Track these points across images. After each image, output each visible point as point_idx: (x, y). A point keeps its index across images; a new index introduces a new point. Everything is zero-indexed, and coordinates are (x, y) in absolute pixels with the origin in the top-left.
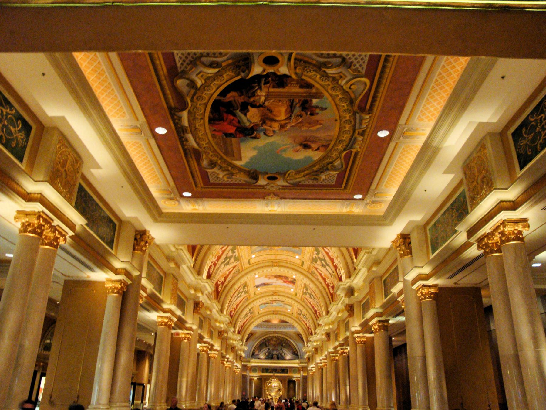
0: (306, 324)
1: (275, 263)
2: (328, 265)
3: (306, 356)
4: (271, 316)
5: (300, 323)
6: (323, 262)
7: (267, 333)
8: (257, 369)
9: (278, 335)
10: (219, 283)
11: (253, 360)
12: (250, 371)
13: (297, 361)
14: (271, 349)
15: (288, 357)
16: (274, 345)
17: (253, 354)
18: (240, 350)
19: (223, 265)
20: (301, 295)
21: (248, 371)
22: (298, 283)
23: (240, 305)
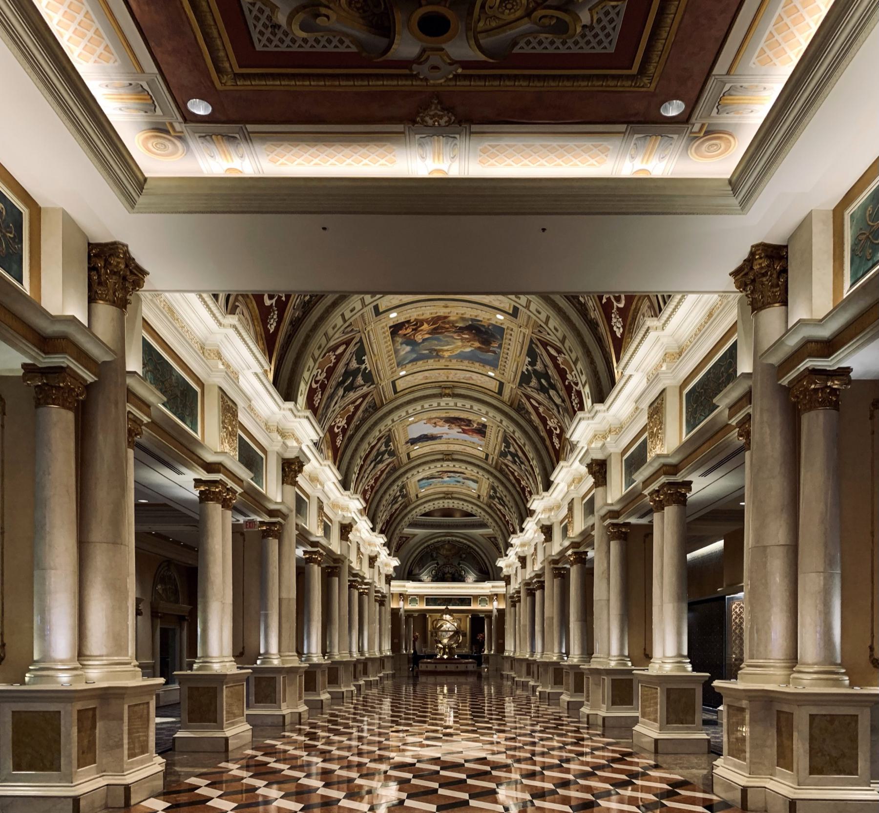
0: (504, 516)
1: (448, 390)
2: (553, 387)
5: (493, 514)
6: (543, 381)
10: (336, 430)
14: (441, 563)
16: (446, 557)
19: (341, 392)
20: (496, 457)
22: (491, 433)
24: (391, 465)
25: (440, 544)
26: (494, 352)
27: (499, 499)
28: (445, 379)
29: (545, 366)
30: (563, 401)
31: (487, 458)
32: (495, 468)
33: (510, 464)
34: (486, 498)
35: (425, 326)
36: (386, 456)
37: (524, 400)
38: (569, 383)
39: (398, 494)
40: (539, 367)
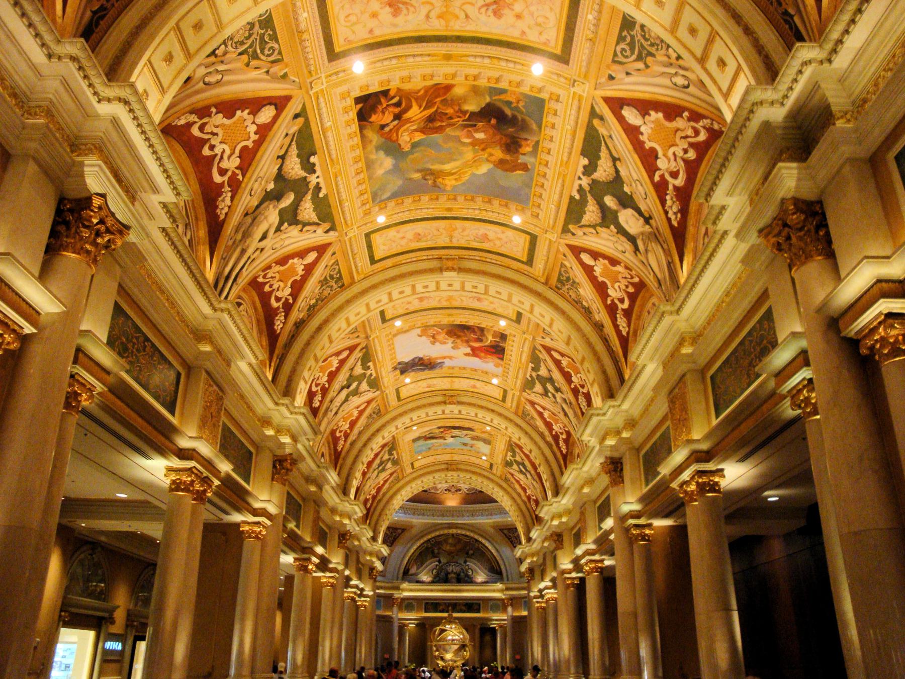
1: (448, 259)
3: (524, 568)
4: (443, 474)
5: (509, 489)
7: (436, 527)
8: (415, 603)
9: (459, 531)
11: (405, 585)
12: (400, 609)
13: (499, 586)
14: (443, 560)
15: (480, 578)
16: (450, 553)
17: (406, 572)
18: (371, 554)
20: (517, 393)
21: (395, 608)
23: (384, 490)
24: (373, 405)
25: (442, 538)
26: (525, 167)
27: (518, 463)
29: (615, 160)
30: (647, 220)
31: (504, 397)
32: (516, 413)
33: (538, 399)
34: (500, 467)
35: (415, 112)
36: (364, 386)
37: (571, 262)
38: (662, 176)
39: (386, 457)
40: (604, 171)
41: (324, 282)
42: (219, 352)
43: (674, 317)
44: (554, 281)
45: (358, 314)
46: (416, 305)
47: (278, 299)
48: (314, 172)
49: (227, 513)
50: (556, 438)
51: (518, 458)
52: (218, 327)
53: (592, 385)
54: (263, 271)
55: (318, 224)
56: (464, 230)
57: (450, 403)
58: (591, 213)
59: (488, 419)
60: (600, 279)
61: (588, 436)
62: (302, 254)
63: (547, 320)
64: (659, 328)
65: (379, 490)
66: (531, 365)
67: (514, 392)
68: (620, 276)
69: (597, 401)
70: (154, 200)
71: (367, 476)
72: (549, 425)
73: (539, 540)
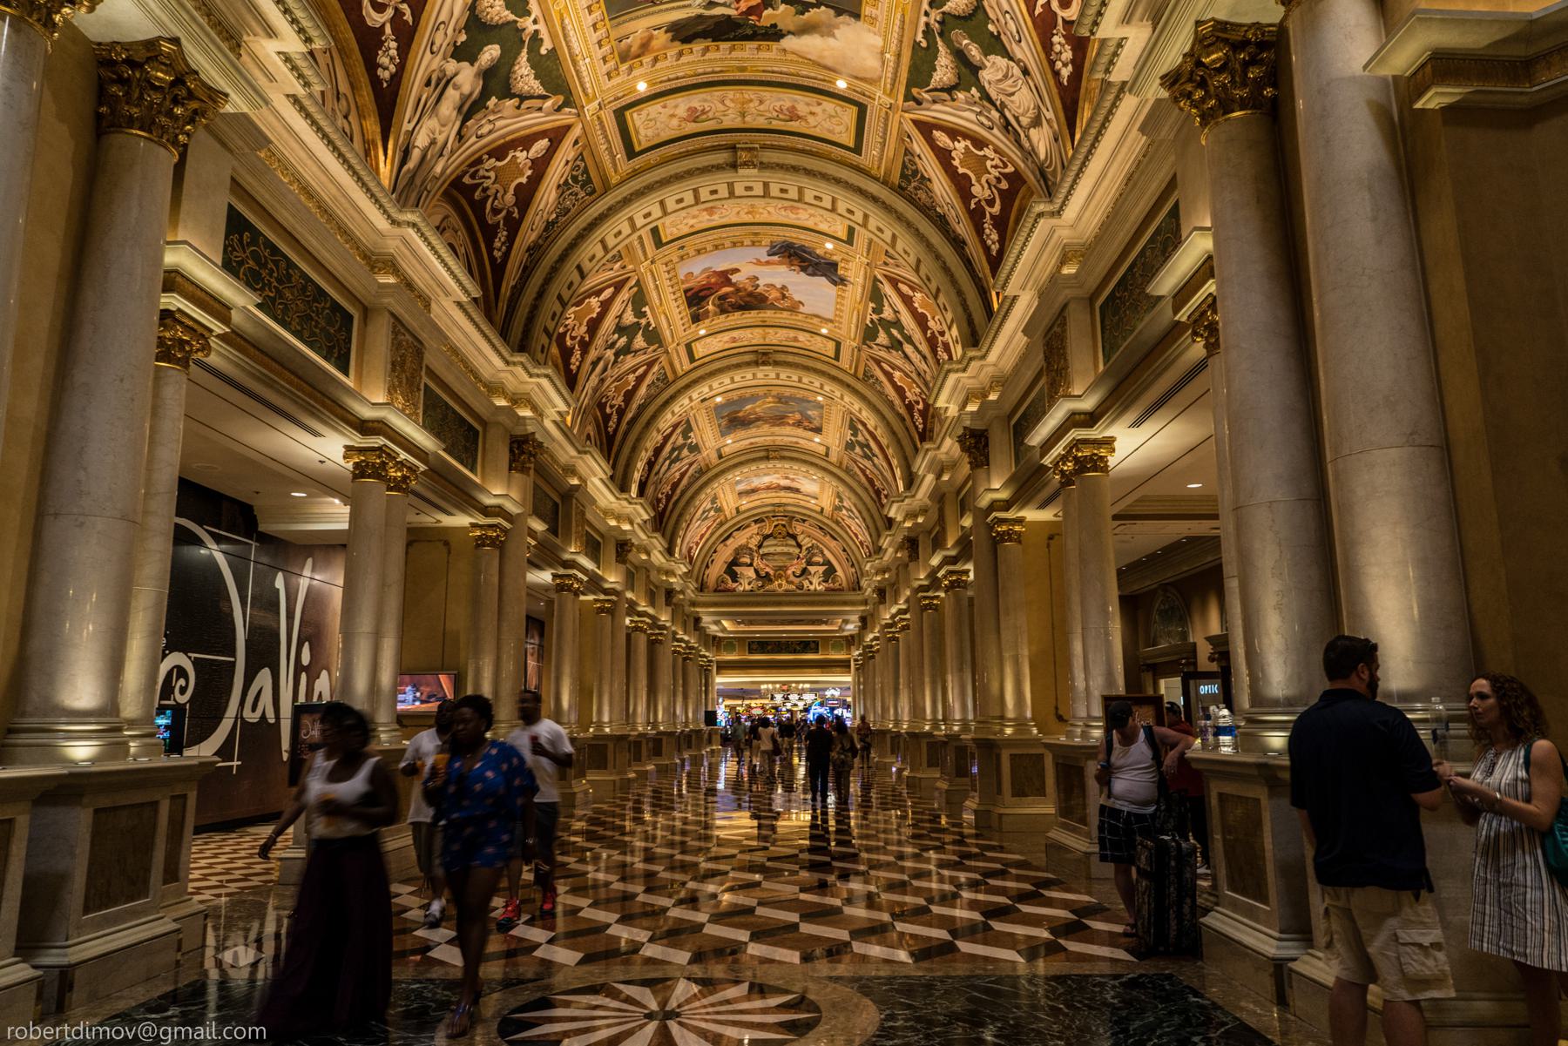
0: (871, 482)
27: (862, 446)
28: (738, 123)
32: (855, 376)
33: (883, 354)
36: (639, 341)
37: (919, 146)
39: (681, 441)
41: (563, 187)
42: (409, 285)
43: (1054, 221)
44: (895, 178)
45: (620, 233)
46: (704, 220)
47: (496, 211)
48: (529, 14)
49: (449, 514)
50: (910, 407)
51: (860, 438)
52: (403, 248)
53: (950, 328)
54: (470, 166)
55: (544, 98)
56: (761, 102)
57: (764, 363)
58: (944, 70)
59: (817, 384)
60: (961, 171)
61: (947, 403)
62: (526, 142)
63: (887, 236)
64: (1032, 240)
65: (675, 486)
66: (872, 305)
67: (849, 345)
68: (989, 163)
69: (958, 351)
70: (268, 49)
71: (657, 468)
72: (900, 391)
73: (891, 550)
